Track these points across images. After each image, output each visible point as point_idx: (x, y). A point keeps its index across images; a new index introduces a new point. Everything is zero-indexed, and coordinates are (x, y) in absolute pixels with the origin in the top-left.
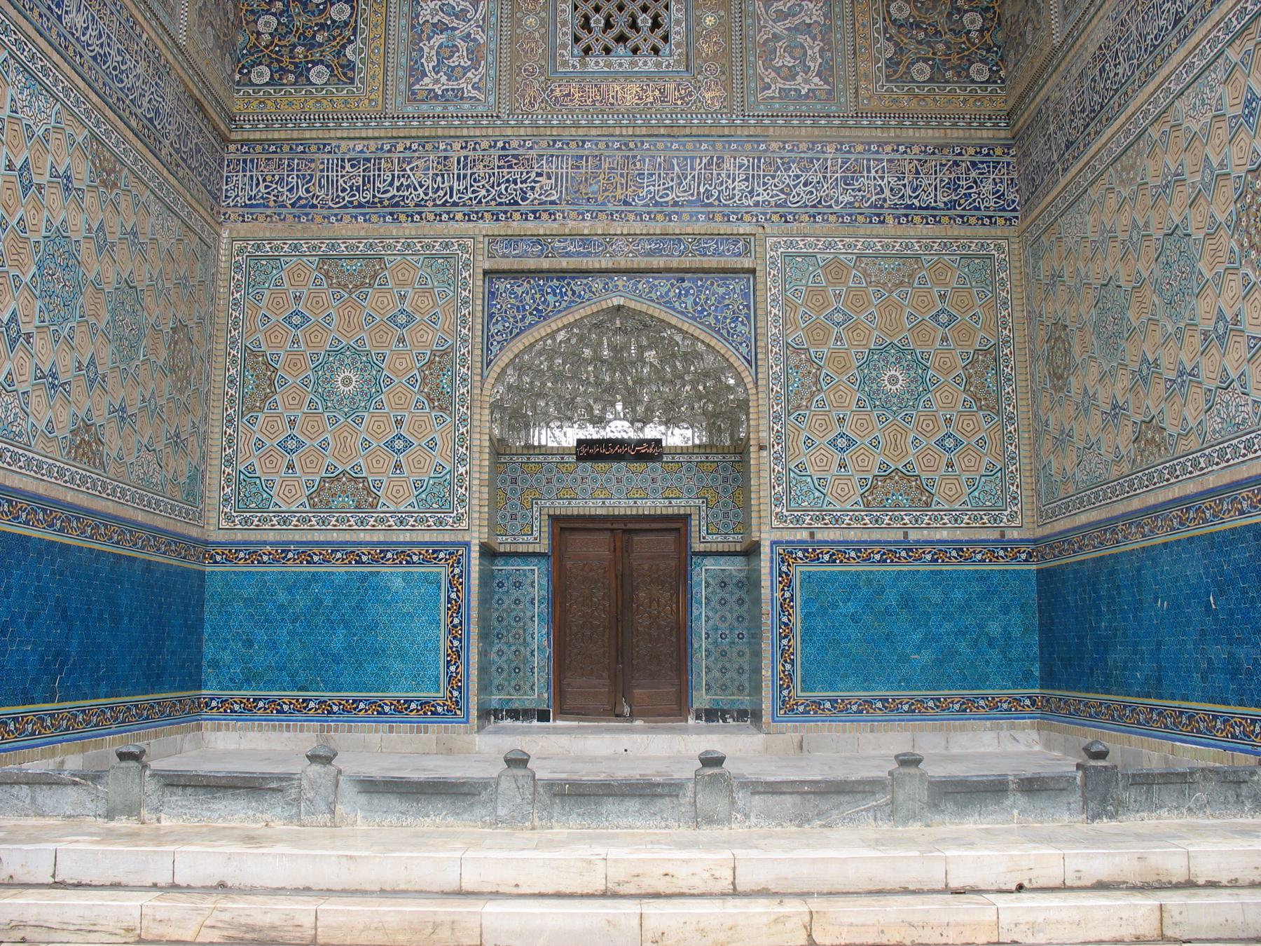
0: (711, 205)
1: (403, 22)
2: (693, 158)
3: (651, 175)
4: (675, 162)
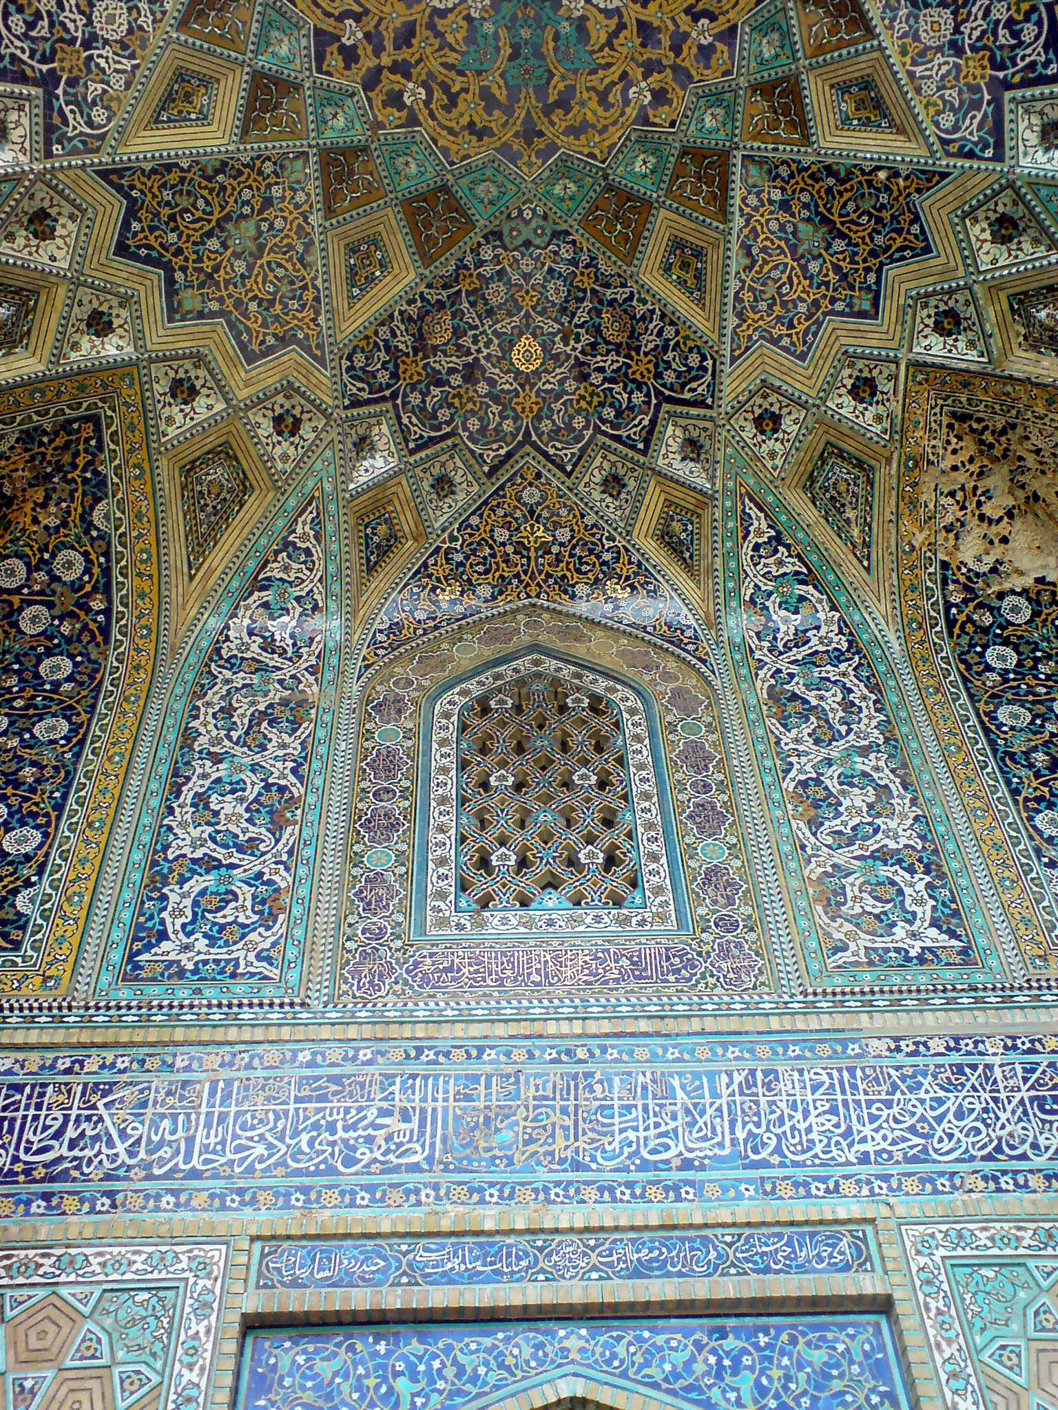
0: (765, 1164)
1: (137, 856)
2: (712, 1075)
3: (629, 1108)
4: (676, 1082)
